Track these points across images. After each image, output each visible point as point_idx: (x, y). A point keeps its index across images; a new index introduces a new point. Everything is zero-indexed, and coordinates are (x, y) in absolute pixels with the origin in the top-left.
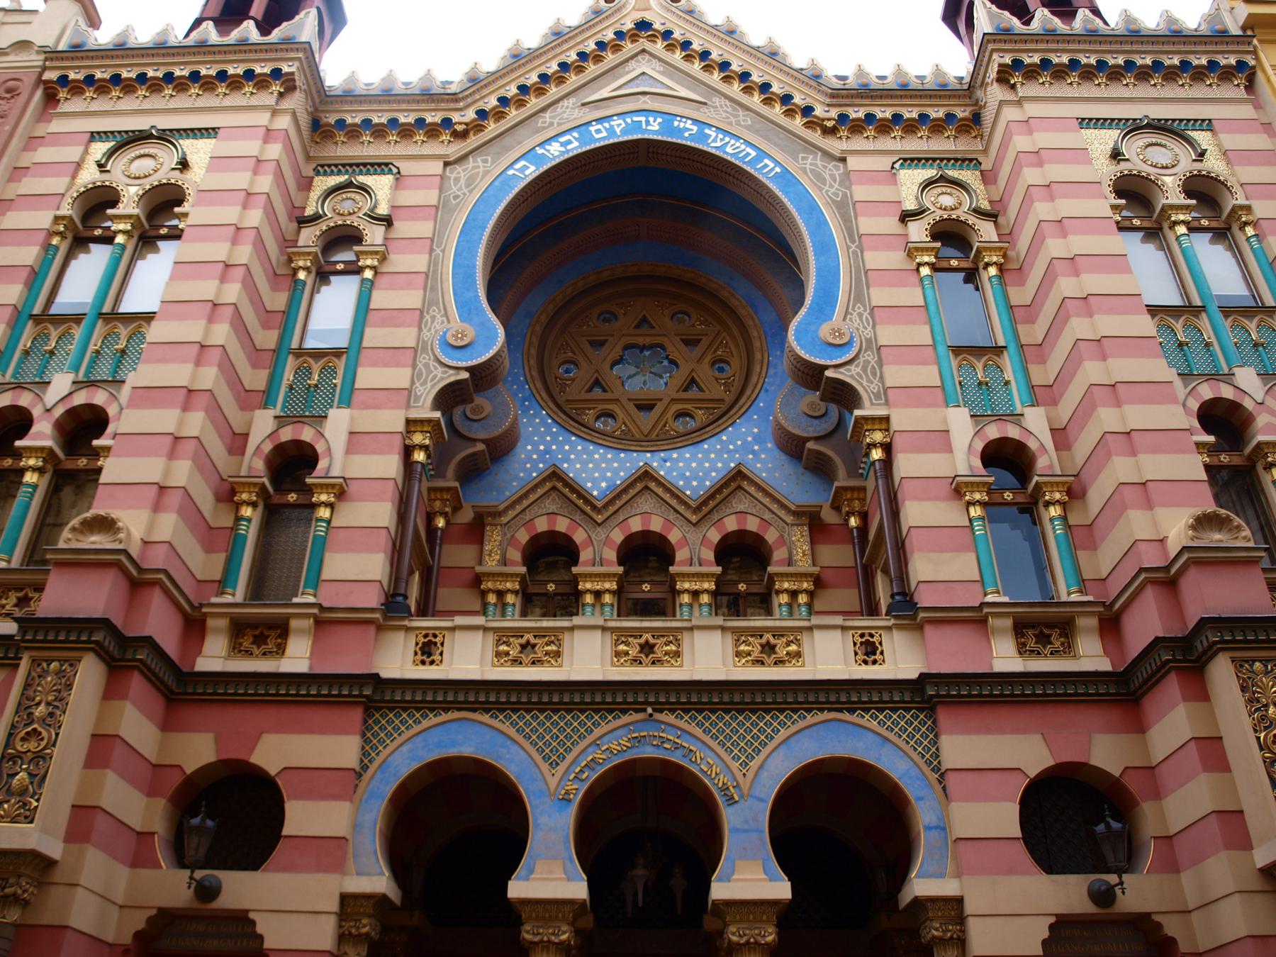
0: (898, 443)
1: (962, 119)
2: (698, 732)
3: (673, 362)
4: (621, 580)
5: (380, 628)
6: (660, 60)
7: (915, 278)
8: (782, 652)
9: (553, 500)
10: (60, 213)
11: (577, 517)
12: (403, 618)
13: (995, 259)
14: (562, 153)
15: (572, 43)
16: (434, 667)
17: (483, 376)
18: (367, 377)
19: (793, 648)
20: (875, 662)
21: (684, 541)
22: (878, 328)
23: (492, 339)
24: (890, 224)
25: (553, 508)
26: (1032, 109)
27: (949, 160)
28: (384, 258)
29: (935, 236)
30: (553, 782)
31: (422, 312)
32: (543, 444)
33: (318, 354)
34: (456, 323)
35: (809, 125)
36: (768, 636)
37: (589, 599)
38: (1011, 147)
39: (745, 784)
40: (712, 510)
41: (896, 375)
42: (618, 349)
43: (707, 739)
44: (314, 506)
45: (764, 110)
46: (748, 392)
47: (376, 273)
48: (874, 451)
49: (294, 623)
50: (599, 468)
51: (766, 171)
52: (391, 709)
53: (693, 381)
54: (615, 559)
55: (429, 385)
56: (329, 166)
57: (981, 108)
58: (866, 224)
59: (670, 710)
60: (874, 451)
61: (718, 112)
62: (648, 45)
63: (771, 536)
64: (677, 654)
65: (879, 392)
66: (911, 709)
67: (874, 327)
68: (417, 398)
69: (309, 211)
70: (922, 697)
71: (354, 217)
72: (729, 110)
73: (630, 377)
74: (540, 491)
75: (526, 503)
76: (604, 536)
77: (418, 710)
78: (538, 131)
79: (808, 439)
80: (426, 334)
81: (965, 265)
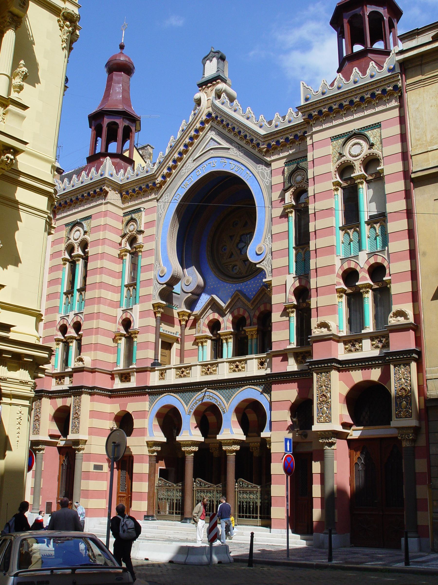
8: (240, 367)
10: (62, 257)
26: (316, 137)
40: (257, 303)
42: (238, 238)
71: (134, 232)
73: (243, 248)
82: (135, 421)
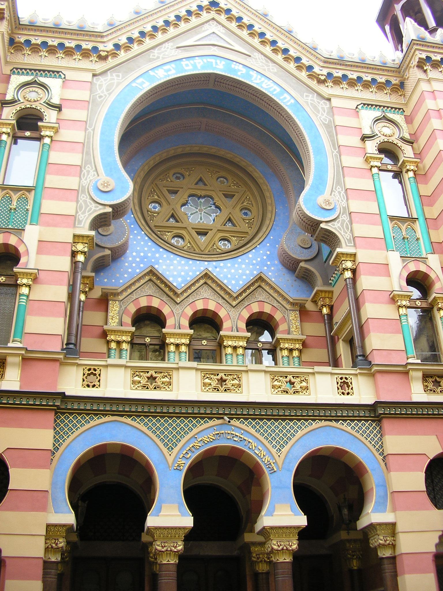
0: (361, 269)
1: (394, 85)
2: (253, 431)
3: (217, 207)
4: (192, 338)
5: (62, 364)
6: (223, 26)
7: (369, 174)
8: (298, 386)
9: (150, 287)
11: (165, 298)
12: (76, 359)
13: (412, 168)
14: (166, 76)
15: (172, 9)
16: (94, 389)
17: (118, 211)
18: (49, 206)
19: (304, 384)
20: (348, 394)
21: (229, 316)
22: (350, 201)
23: (124, 188)
24: (356, 141)
25: (150, 292)
26: (436, 86)
27: (388, 107)
28: (57, 132)
29: (381, 150)
30: (170, 459)
31: (81, 167)
32: (142, 252)
33: (16, 189)
34: (103, 177)
35: (310, 76)
36: (290, 377)
37: (172, 348)
38: (424, 105)
39: (280, 461)
41: (361, 229)
42: (186, 196)
43: (258, 435)
44: (17, 286)
45: (284, 64)
46: (264, 229)
47: (52, 140)
48: (346, 272)
49: (9, 359)
50: (179, 270)
51: (285, 102)
52: (71, 414)
53: (230, 220)
54: (188, 326)
55: (87, 214)
56: (21, 69)
57: (405, 79)
58: (344, 140)
59: (237, 418)
60: (346, 272)
61: (257, 62)
62: (217, 17)
63: (278, 316)
64: (239, 386)
65: (350, 238)
66: (369, 420)
67: (347, 200)
68: (80, 222)
69: (9, 97)
70: (375, 414)
71: (37, 104)
72: (264, 61)
74: (142, 282)
75: (134, 288)
76: (180, 311)
77: (88, 414)
78: (151, 60)
79: (301, 261)
80: (84, 182)
81: (395, 169)
82: (12, 471)
